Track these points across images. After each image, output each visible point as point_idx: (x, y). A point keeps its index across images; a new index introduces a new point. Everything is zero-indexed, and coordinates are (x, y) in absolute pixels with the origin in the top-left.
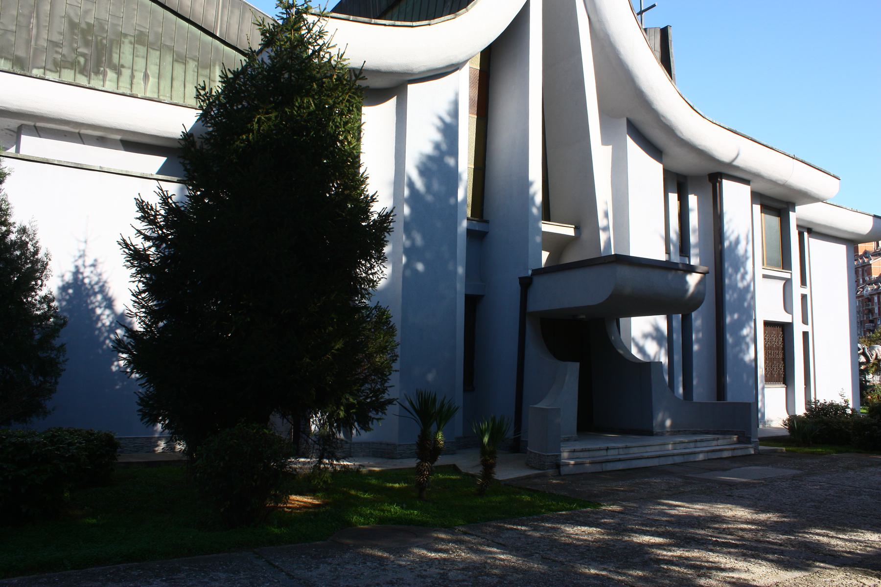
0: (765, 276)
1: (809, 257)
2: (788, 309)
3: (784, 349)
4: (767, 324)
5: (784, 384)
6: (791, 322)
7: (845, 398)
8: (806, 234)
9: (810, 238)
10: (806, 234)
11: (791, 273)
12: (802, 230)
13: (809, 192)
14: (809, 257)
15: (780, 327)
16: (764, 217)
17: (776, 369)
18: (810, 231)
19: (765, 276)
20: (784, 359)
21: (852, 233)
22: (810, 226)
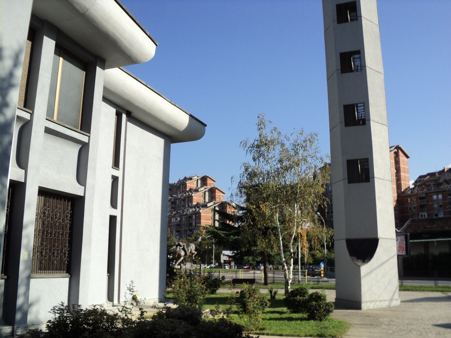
0: (48, 131)
1: (125, 140)
2: (81, 179)
3: (71, 228)
4: (43, 192)
5: (67, 273)
6: (83, 195)
7: (134, 294)
8: (124, 116)
9: (128, 122)
10: (124, 116)
11: (89, 137)
12: (121, 111)
13: (118, 41)
14: (125, 140)
15: (68, 201)
16: (63, 63)
17: (58, 253)
18: (129, 114)
19: (48, 131)
20: (70, 242)
21: (170, 126)
22: (129, 109)
